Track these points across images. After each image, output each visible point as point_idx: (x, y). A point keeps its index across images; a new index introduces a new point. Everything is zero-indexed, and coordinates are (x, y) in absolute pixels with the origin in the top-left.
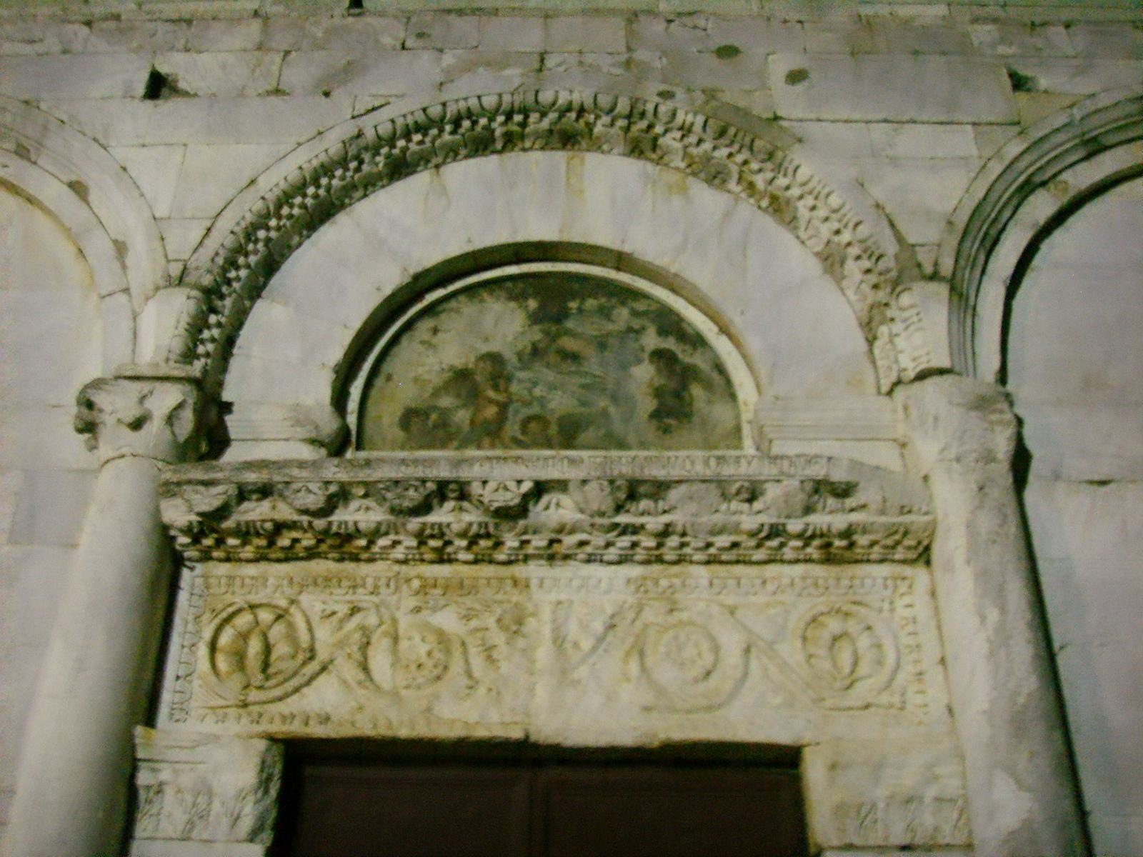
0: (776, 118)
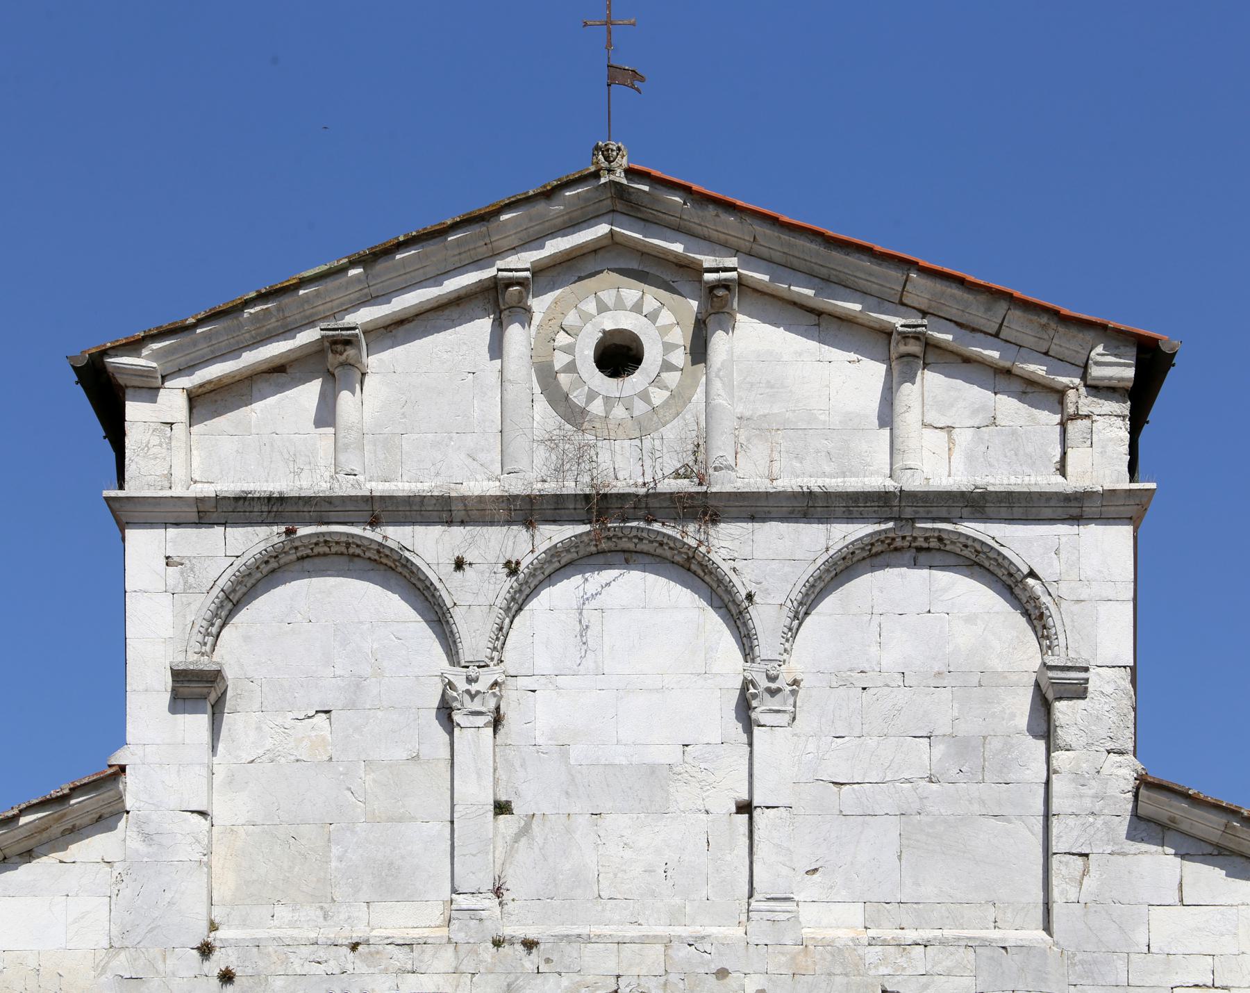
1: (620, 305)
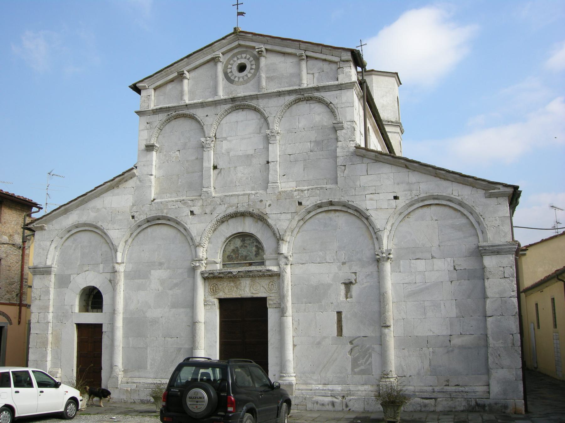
0: (267, 214)
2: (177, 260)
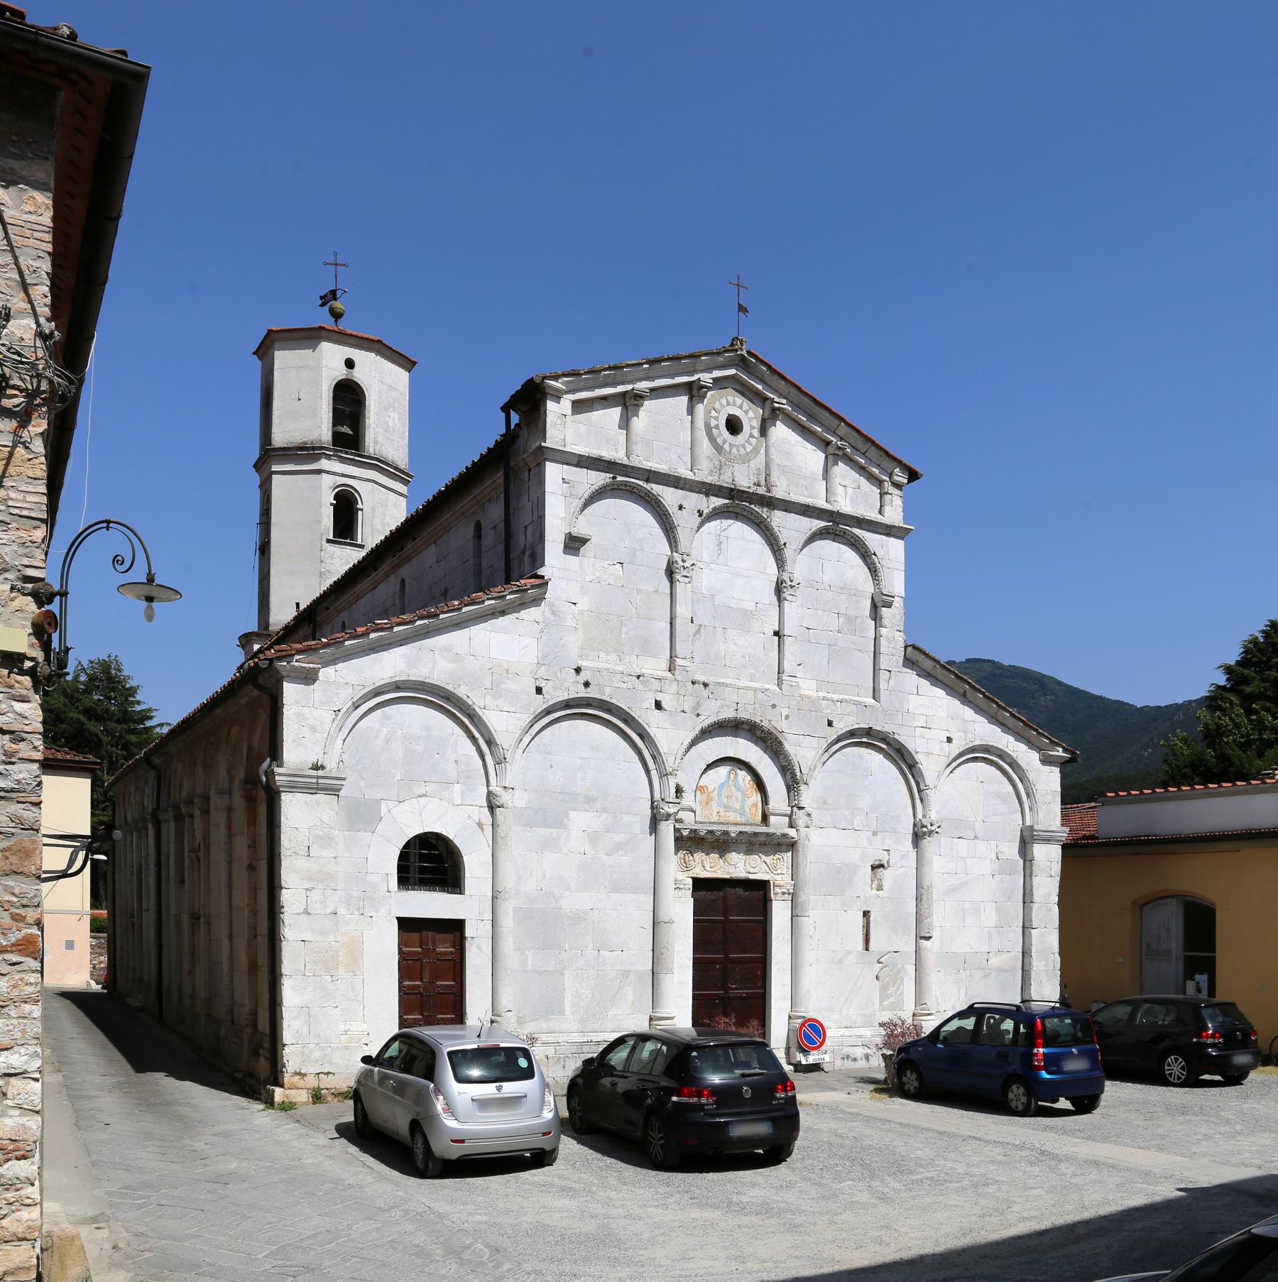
1: (734, 405)
2: (621, 795)
